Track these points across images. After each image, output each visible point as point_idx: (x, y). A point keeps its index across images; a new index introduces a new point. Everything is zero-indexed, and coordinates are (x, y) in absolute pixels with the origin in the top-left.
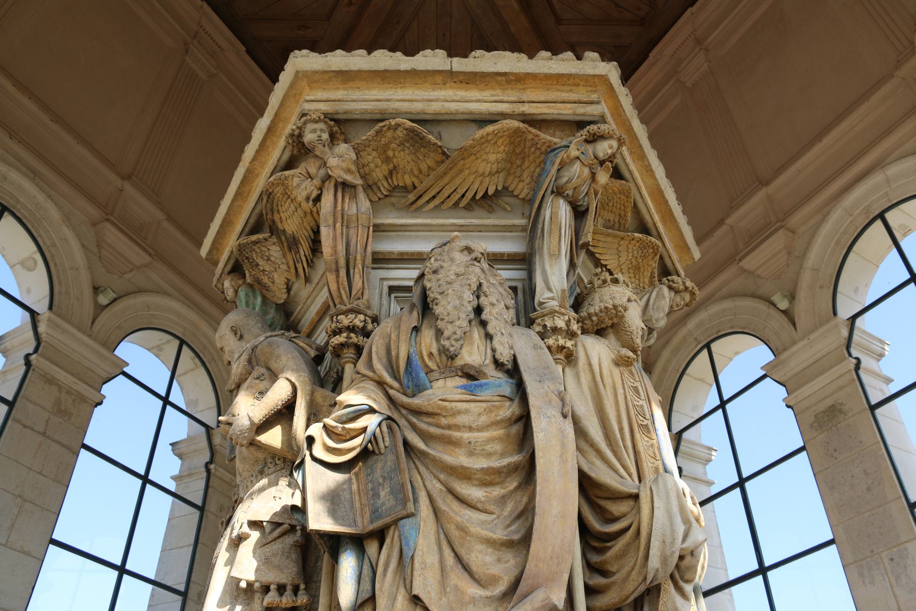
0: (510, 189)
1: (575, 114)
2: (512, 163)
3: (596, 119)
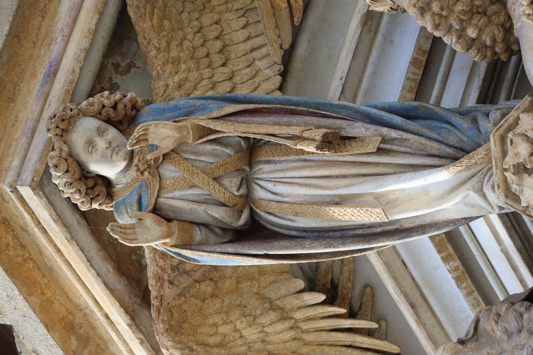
2: (238, 282)
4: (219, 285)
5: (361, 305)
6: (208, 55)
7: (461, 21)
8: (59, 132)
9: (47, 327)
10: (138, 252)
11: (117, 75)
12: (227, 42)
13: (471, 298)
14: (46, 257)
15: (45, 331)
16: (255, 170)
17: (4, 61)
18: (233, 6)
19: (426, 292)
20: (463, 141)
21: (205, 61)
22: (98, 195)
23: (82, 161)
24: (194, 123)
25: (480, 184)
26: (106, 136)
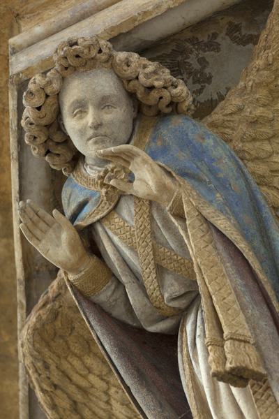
11: (227, 37)
26: (106, 113)
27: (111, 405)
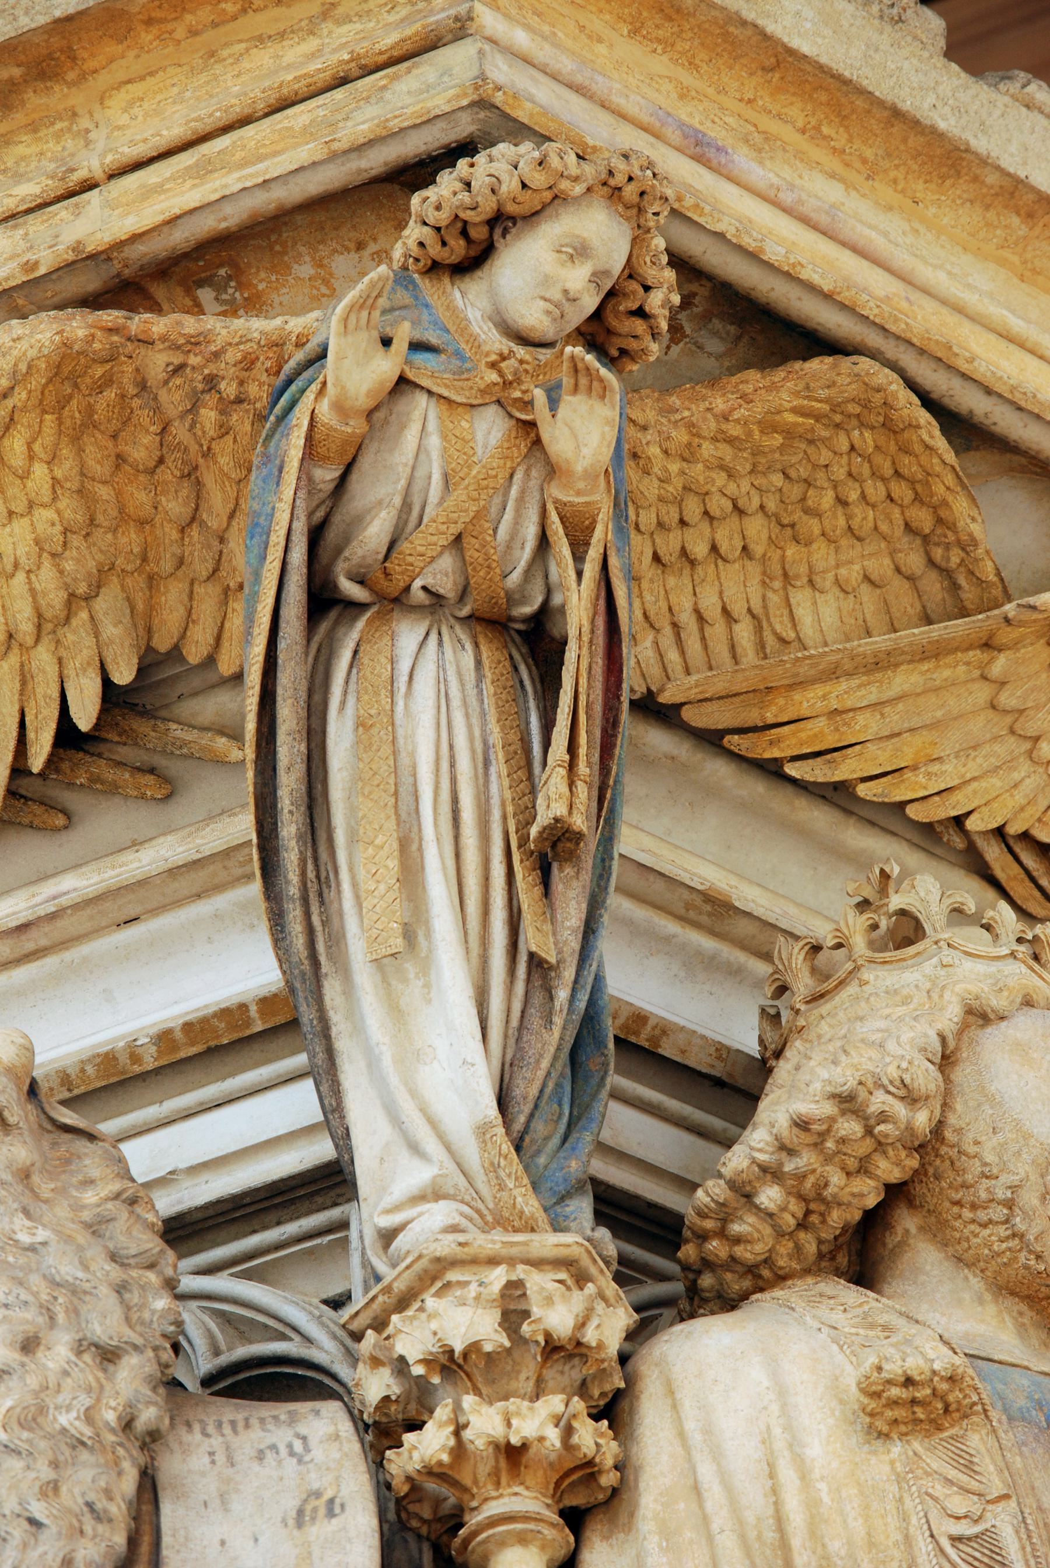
0: (194, 654)
1: (334, 156)
2: (142, 523)
3: (465, 127)
4: (142, 478)
5: (22, 796)
6: (683, 523)
7: (802, 1177)
8: (619, 179)
9: (69, 19)
10: (233, 284)
12: (700, 570)
13: (55, 1083)
14: (247, 50)
15: (58, 13)
16: (458, 629)
17: (731, 29)
18: (774, 591)
19: (50, 962)
20: (538, 1152)
21: (672, 516)
22: (444, 244)
23: (538, 223)
24: (600, 509)
25: (452, 1191)
27: (10, 521)
